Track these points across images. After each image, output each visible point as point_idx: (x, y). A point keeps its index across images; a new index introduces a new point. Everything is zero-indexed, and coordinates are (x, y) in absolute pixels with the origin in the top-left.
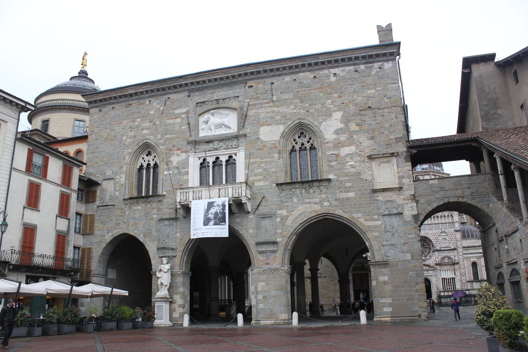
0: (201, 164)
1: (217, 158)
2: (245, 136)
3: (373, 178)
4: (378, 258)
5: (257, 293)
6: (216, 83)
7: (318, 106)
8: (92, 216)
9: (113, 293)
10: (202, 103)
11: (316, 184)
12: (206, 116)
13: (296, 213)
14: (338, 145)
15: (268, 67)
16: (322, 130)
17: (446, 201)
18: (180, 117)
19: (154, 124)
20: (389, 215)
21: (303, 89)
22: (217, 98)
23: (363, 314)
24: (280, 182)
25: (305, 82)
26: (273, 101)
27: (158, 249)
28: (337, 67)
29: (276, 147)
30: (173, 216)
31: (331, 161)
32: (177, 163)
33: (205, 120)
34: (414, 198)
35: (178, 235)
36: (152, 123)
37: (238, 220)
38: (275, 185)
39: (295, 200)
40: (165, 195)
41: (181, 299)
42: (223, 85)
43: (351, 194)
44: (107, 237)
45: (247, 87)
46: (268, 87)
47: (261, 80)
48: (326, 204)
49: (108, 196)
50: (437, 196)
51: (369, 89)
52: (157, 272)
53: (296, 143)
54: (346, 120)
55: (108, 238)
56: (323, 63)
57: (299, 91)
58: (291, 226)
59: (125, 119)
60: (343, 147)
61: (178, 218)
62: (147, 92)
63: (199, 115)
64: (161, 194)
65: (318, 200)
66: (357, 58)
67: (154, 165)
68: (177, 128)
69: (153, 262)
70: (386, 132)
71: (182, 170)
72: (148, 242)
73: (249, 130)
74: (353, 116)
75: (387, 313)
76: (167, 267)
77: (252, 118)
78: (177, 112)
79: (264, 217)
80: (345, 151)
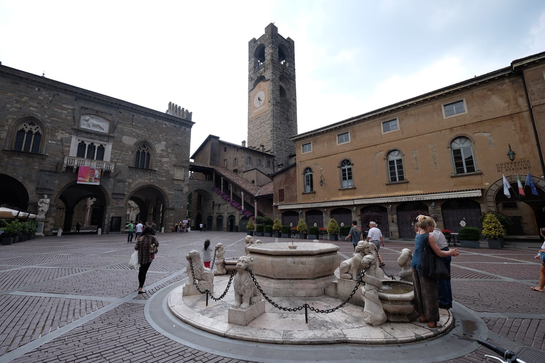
0: (79, 143)
1: (92, 144)
2: (114, 137)
4: (170, 206)
7: (156, 136)
9: (29, 217)
10: (85, 108)
11: (149, 171)
12: (88, 117)
13: (137, 182)
14: (162, 156)
15: (134, 107)
16: (156, 147)
17: (199, 188)
18: (67, 110)
19: (42, 107)
20: (178, 190)
21: (149, 125)
22: (98, 110)
23: (163, 228)
24: (131, 166)
25: (151, 122)
26: (133, 125)
27: (37, 189)
28: (168, 121)
30: (54, 170)
31: (157, 162)
33: (86, 119)
35: (56, 182)
36: (40, 105)
39: (137, 176)
41: (53, 220)
43: (164, 179)
45: (118, 112)
47: (128, 112)
48: (152, 181)
50: (196, 186)
51: (179, 136)
52: (39, 204)
53: (140, 149)
54: (167, 147)
57: (147, 125)
58: (133, 188)
59: (10, 92)
60: (164, 157)
61: (58, 172)
63: (82, 114)
64: (43, 153)
65: (148, 178)
66: (177, 122)
67: (36, 133)
68: (63, 116)
70: (182, 157)
71: (65, 144)
72: (27, 183)
73: (116, 135)
74: (170, 146)
76: (48, 201)
77: (119, 129)
78: (64, 106)
79: (119, 181)
80: (165, 160)
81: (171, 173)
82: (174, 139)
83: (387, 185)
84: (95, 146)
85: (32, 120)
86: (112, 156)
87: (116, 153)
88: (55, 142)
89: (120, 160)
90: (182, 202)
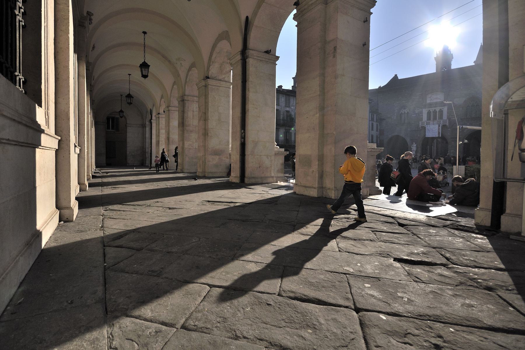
0: (428, 112)
84: (437, 111)
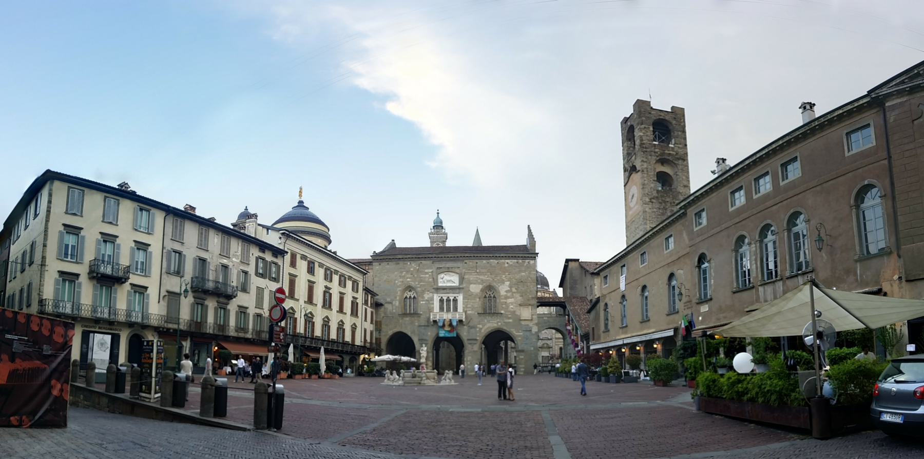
1: (448, 297)
2: (463, 288)
3: (520, 315)
5: (467, 361)
6: (448, 258)
7: (498, 278)
8: (380, 322)
12: (442, 275)
13: (486, 327)
14: (507, 297)
20: (526, 331)
27: (419, 340)
29: (478, 296)
30: (426, 324)
32: (428, 298)
34: (537, 324)
36: (412, 276)
37: (459, 328)
38: (476, 313)
40: (421, 314)
42: (452, 260)
43: (511, 321)
44: (389, 333)
46: (475, 264)
48: (499, 324)
49: (388, 311)
54: (511, 287)
55: (390, 333)
56: (502, 257)
62: (409, 258)
64: (419, 312)
68: (427, 280)
69: (416, 346)
70: (528, 294)
71: (431, 302)
75: (522, 371)
76: (425, 348)
78: (426, 271)
81: (518, 313)
82: (518, 276)
83: (641, 322)
85: (410, 288)
86: (464, 306)
87: (466, 302)
88: (424, 302)
89: (470, 308)
90: (531, 343)
